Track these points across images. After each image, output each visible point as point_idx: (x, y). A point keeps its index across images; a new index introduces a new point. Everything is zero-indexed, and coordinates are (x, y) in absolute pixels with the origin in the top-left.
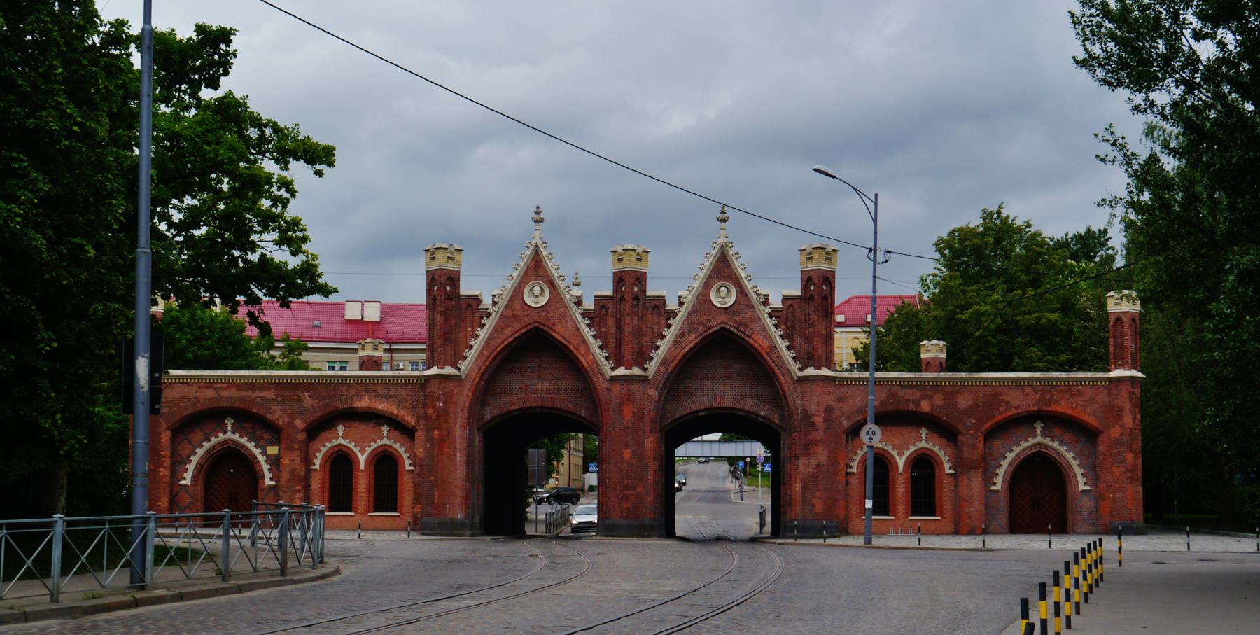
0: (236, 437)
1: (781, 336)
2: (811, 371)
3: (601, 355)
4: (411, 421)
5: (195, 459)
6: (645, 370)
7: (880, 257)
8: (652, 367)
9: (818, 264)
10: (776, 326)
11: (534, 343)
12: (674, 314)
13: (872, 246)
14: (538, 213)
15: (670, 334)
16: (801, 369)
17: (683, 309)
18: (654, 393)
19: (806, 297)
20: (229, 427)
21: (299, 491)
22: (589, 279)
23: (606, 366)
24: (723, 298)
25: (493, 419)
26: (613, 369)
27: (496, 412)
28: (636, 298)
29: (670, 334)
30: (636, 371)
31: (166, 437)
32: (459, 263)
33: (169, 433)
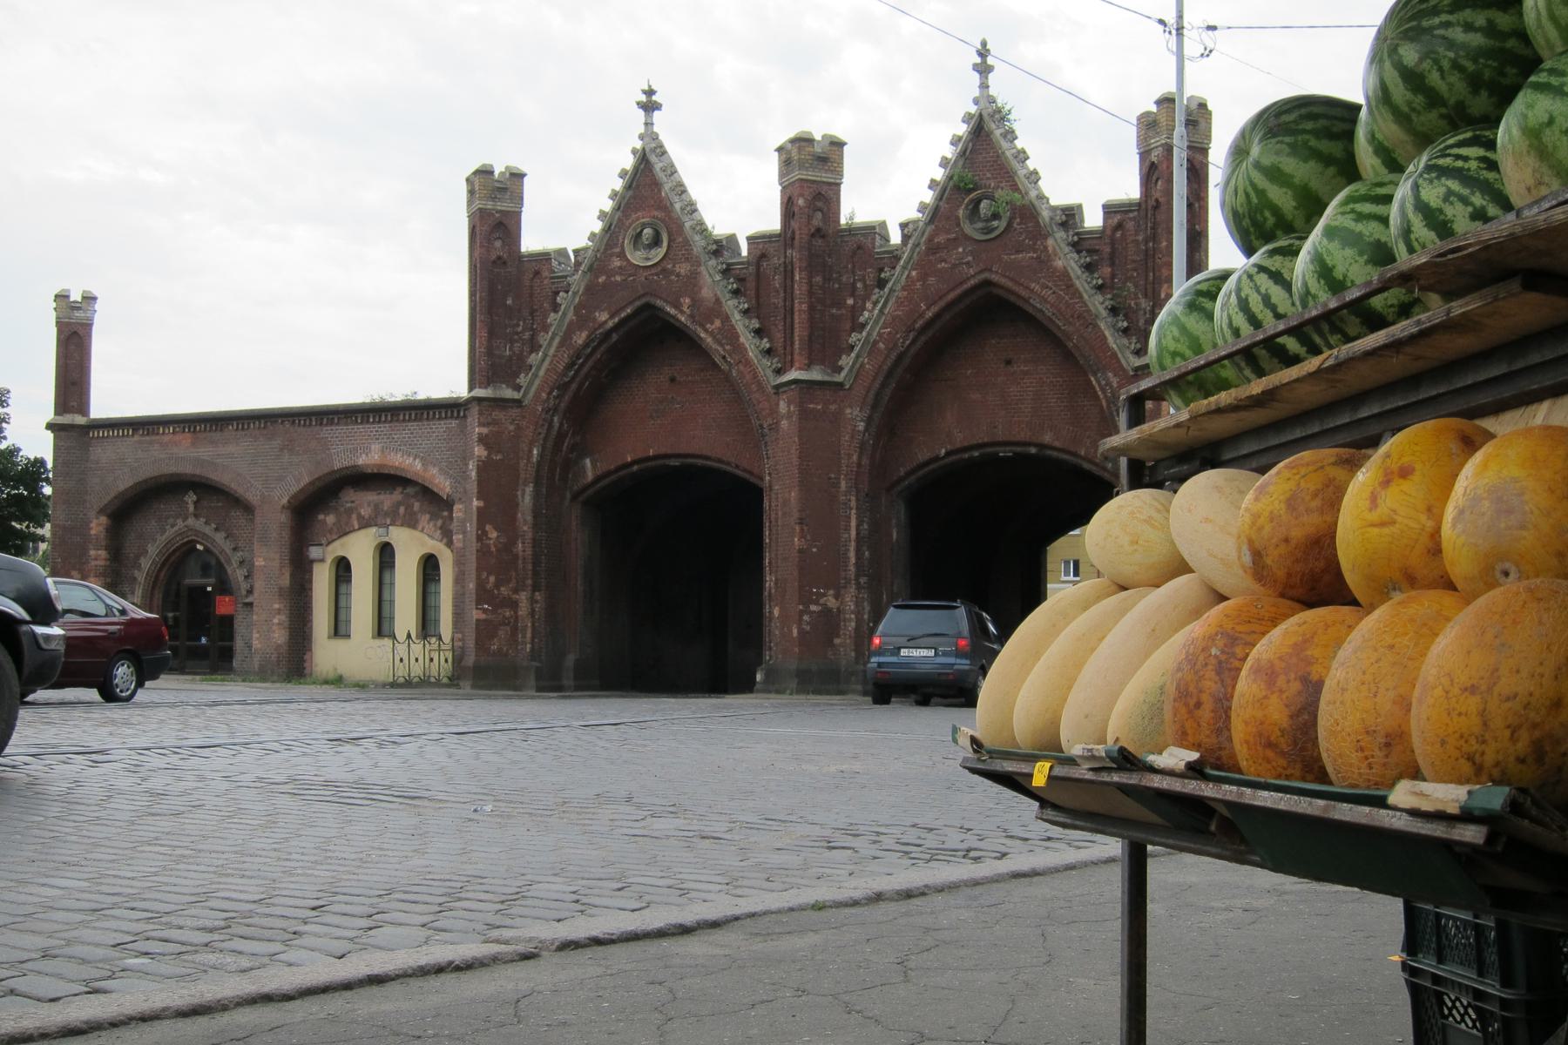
0: (198, 524)
4: (443, 484)
5: (146, 564)
7: (1192, 47)
13: (1171, 19)
14: (650, 92)
18: (855, 417)
20: (191, 508)
21: (279, 611)
22: (737, 201)
25: (598, 479)
26: (779, 372)
27: (603, 467)
31: (98, 526)
32: (519, 199)
33: (104, 519)
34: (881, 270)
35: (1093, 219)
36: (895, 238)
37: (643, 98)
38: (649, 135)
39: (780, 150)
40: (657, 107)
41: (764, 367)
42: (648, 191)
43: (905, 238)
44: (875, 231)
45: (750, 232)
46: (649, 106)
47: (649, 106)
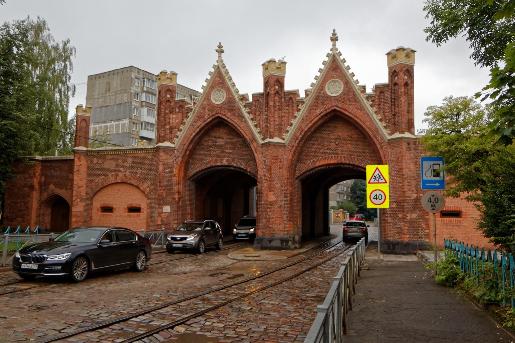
1: (376, 112)
2: (397, 135)
3: (255, 131)
6: (284, 139)
8: (287, 137)
9: (402, 59)
10: (372, 106)
11: (218, 125)
12: (302, 102)
15: (299, 115)
16: (391, 134)
17: (308, 98)
19: (393, 84)
22: (249, 83)
23: (259, 137)
24: (335, 90)
26: (263, 139)
28: (277, 93)
29: (299, 115)
30: (277, 140)
34: (298, 106)
35: (369, 90)
36: (302, 95)
37: (217, 48)
38: (220, 61)
39: (263, 65)
40: (223, 52)
41: (259, 137)
42: (220, 79)
43: (307, 95)
44: (295, 93)
45: (253, 93)
46: (220, 50)
47: (220, 50)
